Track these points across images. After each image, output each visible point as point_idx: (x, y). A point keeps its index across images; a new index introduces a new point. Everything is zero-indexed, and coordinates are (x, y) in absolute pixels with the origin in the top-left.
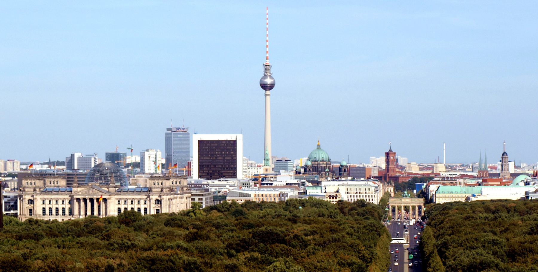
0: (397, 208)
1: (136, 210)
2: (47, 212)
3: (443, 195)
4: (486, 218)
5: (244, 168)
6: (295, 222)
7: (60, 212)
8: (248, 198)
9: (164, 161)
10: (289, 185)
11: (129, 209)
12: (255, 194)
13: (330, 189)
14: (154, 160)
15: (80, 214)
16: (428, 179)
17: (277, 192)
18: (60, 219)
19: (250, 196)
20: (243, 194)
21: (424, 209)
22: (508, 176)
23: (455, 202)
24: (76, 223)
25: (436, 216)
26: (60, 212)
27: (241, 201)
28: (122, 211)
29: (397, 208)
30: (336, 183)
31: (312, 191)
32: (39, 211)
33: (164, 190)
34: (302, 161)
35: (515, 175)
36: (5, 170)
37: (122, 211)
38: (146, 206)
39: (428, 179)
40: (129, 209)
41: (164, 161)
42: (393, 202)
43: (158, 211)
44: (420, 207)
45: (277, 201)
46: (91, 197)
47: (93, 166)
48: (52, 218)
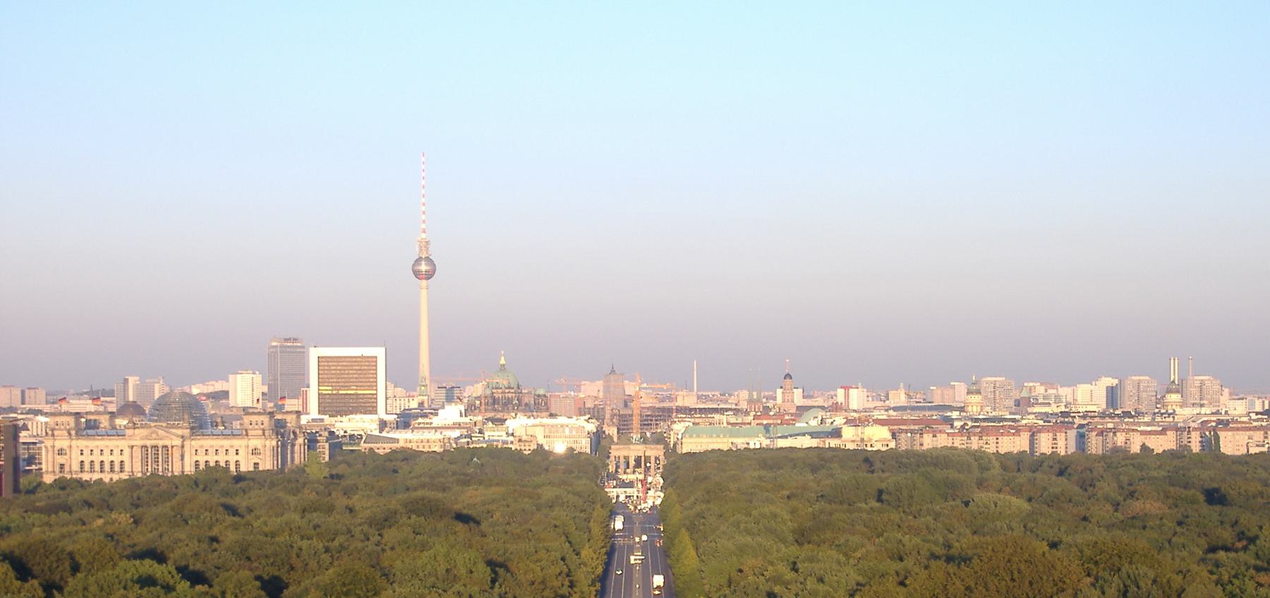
0: (622, 460)
1: (223, 464)
2: (87, 467)
3: (694, 440)
4: (760, 478)
5: (389, 400)
6: (466, 481)
7: (107, 467)
8: (394, 446)
9: (265, 389)
10: (458, 426)
11: (212, 464)
12: (405, 438)
13: (521, 430)
14: (245, 389)
15: (135, 468)
16: (666, 414)
17: (438, 436)
18: (106, 478)
19: (397, 441)
20: (630, 429)
21: (663, 461)
22: (794, 411)
23: (713, 451)
24: (133, 484)
25: (684, 472)
26: (107, 467)
27: (383, 449)
28: (202, 466)
29: (622, 460)
30: (532, 421)
31: (495, 435)
32: (76, 467)
33: (267, 433)
34: (477, 390)
35: (802, 410)
36: (23, 403)
37: (202, 466)
38: (237, 458)
39: (666, 414)
40: (212, 464)
41: (265, 389)
42: (617, 452)
43: (256, 464)
44: (657, 458)
45: (438, 449)
46: (154, 442)
47: (157, 397)
48: (96, 476)
